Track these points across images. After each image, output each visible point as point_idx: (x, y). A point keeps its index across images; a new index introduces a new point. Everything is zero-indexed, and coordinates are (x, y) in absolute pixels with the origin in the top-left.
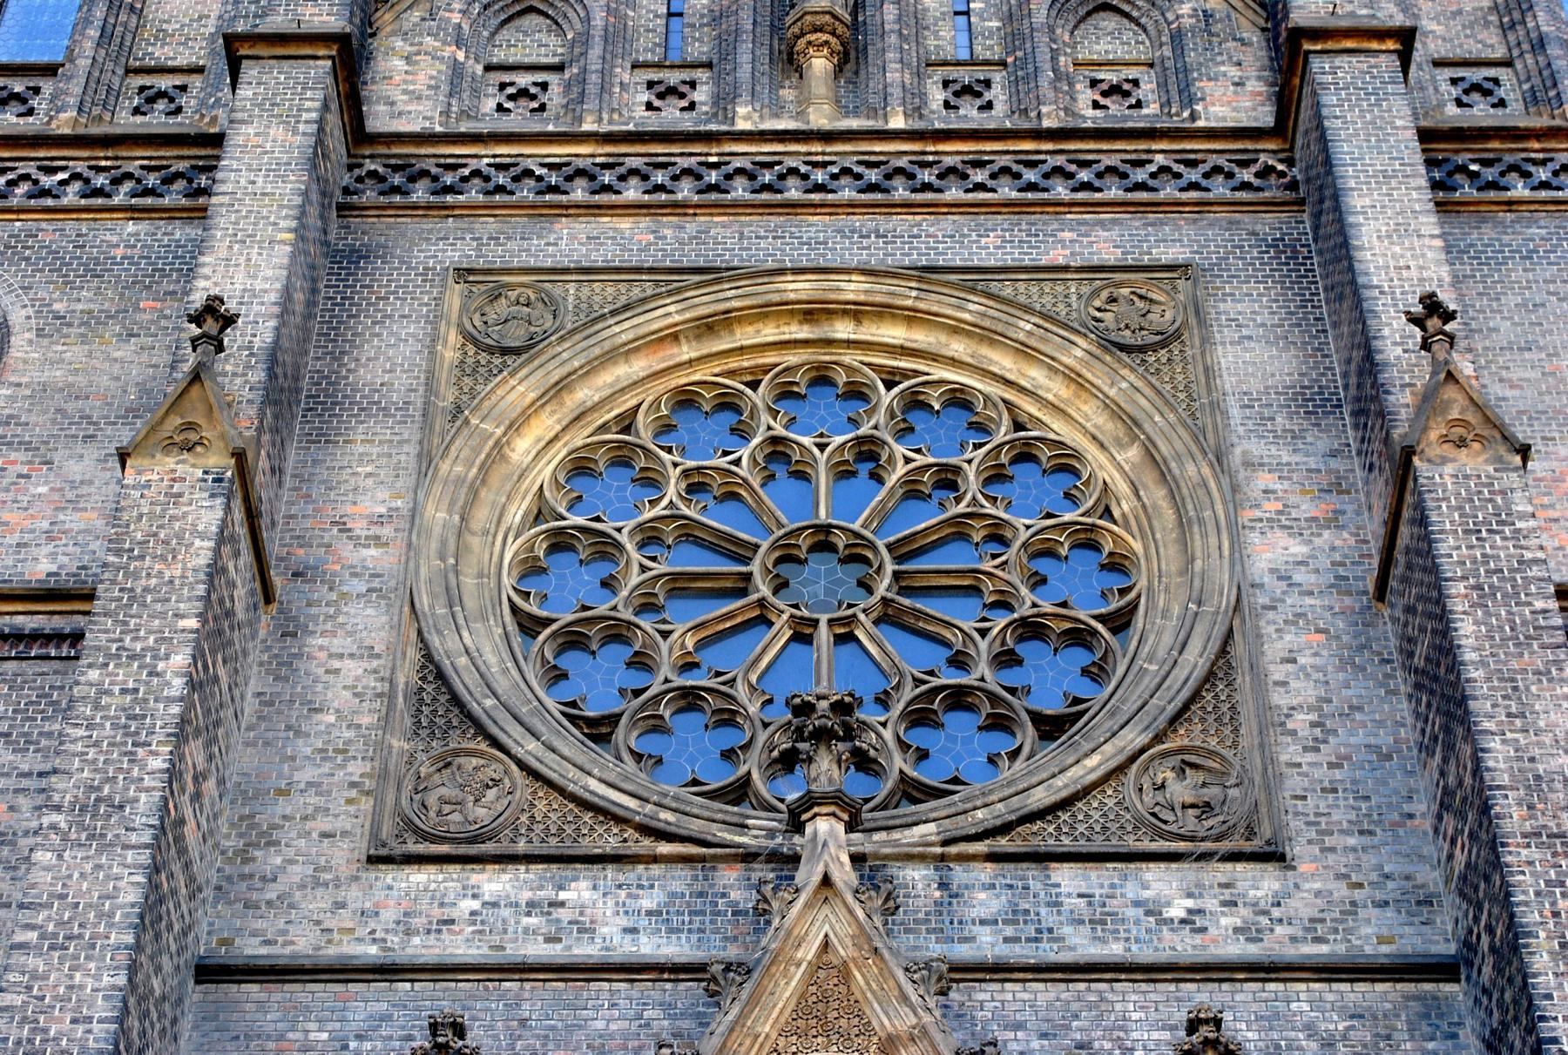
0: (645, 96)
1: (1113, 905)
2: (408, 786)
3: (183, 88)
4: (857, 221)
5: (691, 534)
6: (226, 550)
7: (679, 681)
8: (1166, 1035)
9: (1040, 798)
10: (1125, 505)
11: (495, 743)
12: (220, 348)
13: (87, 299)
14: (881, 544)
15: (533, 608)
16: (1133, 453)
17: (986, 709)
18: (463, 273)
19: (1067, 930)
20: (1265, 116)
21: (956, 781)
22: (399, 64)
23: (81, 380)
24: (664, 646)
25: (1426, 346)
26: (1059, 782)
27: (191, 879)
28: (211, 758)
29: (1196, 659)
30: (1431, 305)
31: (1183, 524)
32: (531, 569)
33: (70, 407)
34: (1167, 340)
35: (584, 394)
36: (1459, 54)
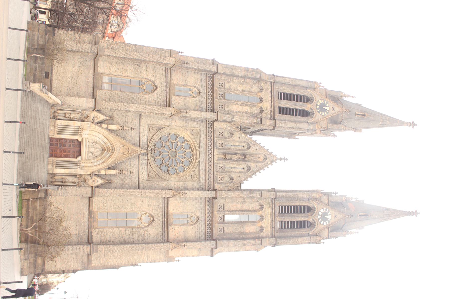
4: (205, 158)
9: (152, 166)
10: (178, 175)
16: (183, 176)
22: (223, 124)
29: (163, 177)
35: (189, 138)
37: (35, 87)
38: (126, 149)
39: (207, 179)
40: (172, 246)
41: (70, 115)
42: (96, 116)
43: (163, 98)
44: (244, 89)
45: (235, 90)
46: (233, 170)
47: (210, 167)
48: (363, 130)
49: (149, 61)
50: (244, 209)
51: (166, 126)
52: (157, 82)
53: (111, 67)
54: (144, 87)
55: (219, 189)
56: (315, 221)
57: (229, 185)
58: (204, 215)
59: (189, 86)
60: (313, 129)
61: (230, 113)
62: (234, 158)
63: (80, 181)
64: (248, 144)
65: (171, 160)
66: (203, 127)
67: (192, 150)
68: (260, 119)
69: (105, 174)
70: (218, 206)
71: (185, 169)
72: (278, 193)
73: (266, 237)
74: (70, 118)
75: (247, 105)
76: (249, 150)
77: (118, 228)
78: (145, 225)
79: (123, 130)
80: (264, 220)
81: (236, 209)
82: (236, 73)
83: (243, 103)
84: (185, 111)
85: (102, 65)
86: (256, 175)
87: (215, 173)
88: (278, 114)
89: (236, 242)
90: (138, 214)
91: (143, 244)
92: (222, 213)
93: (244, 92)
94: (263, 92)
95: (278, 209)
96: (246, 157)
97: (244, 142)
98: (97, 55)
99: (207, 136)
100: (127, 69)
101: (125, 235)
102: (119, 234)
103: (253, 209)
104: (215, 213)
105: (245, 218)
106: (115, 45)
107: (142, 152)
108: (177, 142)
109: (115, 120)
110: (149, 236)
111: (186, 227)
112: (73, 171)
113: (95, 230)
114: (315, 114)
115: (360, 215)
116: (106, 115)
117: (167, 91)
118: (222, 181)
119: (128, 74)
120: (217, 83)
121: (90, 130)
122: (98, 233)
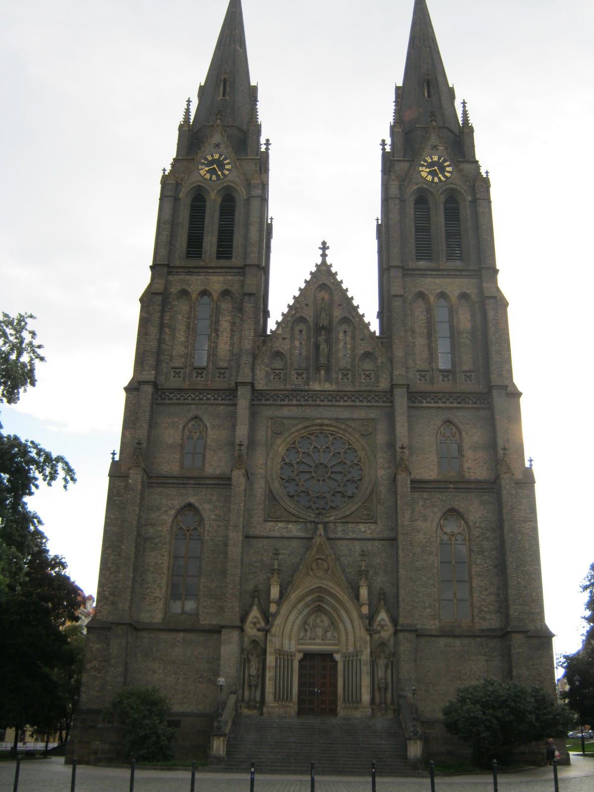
0: (295, 376)
1: (355, 529)
4: (328, 408)
8: (359, 548)
9: (348, 513)
10: (362, 460)
11: (279, 503)
19: (349, 533)
21: (338, 506)
26: (350, 510)
29: (369, 491)
35: (289, 439)
37: (218, 746)
38: (318, 563)
39: (369, 404)
40: (506, 473)
41: (253, 676)
42: (252, 625)
44: (184, 327)
45: (186, 347)
46: (349, 352)
47: (346, 399)
48: (253, 83)
49: (139, 520)
50: (425, 331)
51: (267, 485)
52: (178, 503)
53: (151, 596)
54: (188, 530)
55: (388, 379)
56: (444, 188)
57: (379, 361)
59: (182, 439)
60: (261, 188)
61: (236, 356)
63: (382, 655)
64: (295, 321)
65: (332, 476)
66: (268, 412)
67: (313, 434)
68: (246, 298)
69: (369, 605)
70: (422, 382)
71: (350, 448)
72: (393, 264)
73: (481, 289)
75: (217, 322)
76: (308, 319)
77: (471, 580)
78: (464, 528)
79: (279, 571)
80: (447, 292)
82: (154, 344)
84: (237, 448)
85: (148, 615)
86: (358, 307)
87: (357, 388)
88: (233, 259)
90: (442, 540)
91: (505, 530)
92: (435, 376)
93: (191, 327)
94: (189, 289)
95: (422, 264)
96: (323, 325)
97: (292, 329)
98: (131, 624)
99: (283, 403)
100: (153, 564)
101: (486, 565)
102: (483, 578)
103: (425, 313)
104: (435, 388)
105: (443, 330)
106: (105, 588)
107: (323, 533)
108: (298, 463)
110: (484, 519)
111: (466, 446)
112: (366, 669)
113: (478, 624)
114: (230, 184)
115: (429, 97)
116: (251, 606)
117: (196, 484)
118: (372, 375)
119: (164, 561)
120: (175, 382)
121: (282, 637)
122: (483, 619)
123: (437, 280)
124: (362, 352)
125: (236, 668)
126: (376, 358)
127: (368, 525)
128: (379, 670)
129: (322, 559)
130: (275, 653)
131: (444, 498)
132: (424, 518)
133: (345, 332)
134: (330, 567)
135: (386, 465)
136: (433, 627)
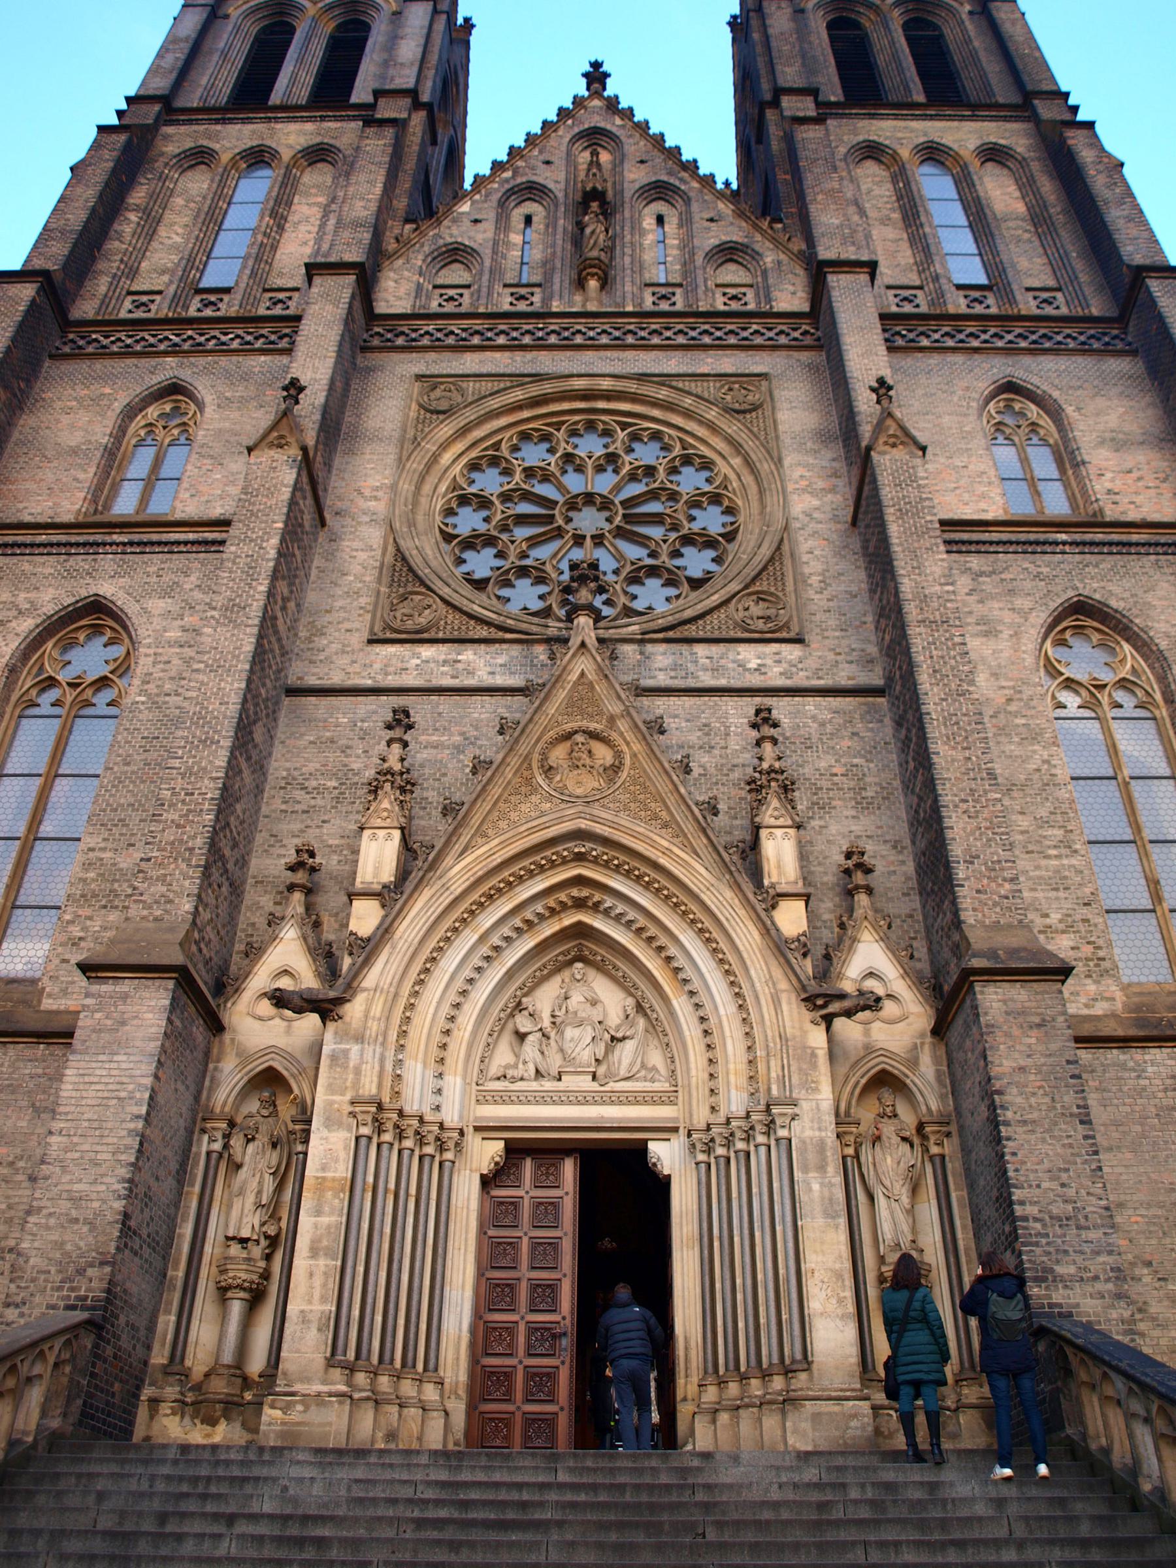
0: (510, 299)
1: (722, 662)
2: (387, 608)
3: (290, 298)
4: (609, 354)
5: (527, 496)
6: (298, 494)
7: (518, 563)
9: (689, 614)
11: (429, 589)
12: (297, 402)
13: (240, 391)
14: (617, 502)
15: (450, 530)
17: (666, 576)
18: (419, 377)
20: (805, 307)
22: (391, 284)
23: (238, 427)
24: (512, 547)
25: (878, 402)
26: (699, 606)
27: (282, 647)
28: (291, 592)
29: (766, 551)
30: (881, 381)
31: (761, 492)
32: (450, 512)
33: (232, 439)
34: (755, 408)
36: (898, 283)
41: (243, 1241)
42: (266, 1008)
43: (178, 561)
50: (896, 216)
58: (976, 356)
62: (602, 237)
63: (888, 1129)
64: (511, 192)
67: (558, 426)
74: (273, 1241)
76: (551, 186)
81: (905, 246)
83: (268, 213)
89: (1115, 216)
96: (594, 189)
103: (890, 186)
109: (318, 860)
117: (131, 544)
123: (914, 124)
124: (714, 242)
125: (124, 1172)
126: (756, 256)
127: (775, 647)
128: (881, 1202)
129: (594, 735)
130: (353, 1114)
131: (1045, 570)
132: (984, 628)
133: (660, 220)
134: (627, 761)
135: (820, 484)
136: (1100, 1009)
